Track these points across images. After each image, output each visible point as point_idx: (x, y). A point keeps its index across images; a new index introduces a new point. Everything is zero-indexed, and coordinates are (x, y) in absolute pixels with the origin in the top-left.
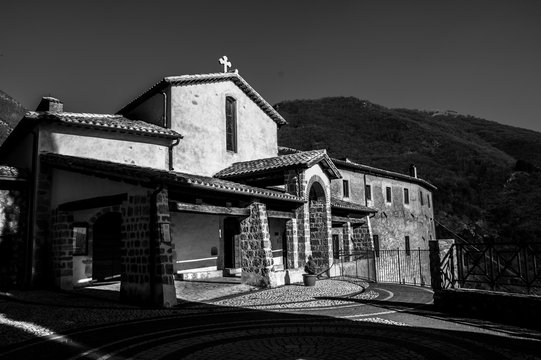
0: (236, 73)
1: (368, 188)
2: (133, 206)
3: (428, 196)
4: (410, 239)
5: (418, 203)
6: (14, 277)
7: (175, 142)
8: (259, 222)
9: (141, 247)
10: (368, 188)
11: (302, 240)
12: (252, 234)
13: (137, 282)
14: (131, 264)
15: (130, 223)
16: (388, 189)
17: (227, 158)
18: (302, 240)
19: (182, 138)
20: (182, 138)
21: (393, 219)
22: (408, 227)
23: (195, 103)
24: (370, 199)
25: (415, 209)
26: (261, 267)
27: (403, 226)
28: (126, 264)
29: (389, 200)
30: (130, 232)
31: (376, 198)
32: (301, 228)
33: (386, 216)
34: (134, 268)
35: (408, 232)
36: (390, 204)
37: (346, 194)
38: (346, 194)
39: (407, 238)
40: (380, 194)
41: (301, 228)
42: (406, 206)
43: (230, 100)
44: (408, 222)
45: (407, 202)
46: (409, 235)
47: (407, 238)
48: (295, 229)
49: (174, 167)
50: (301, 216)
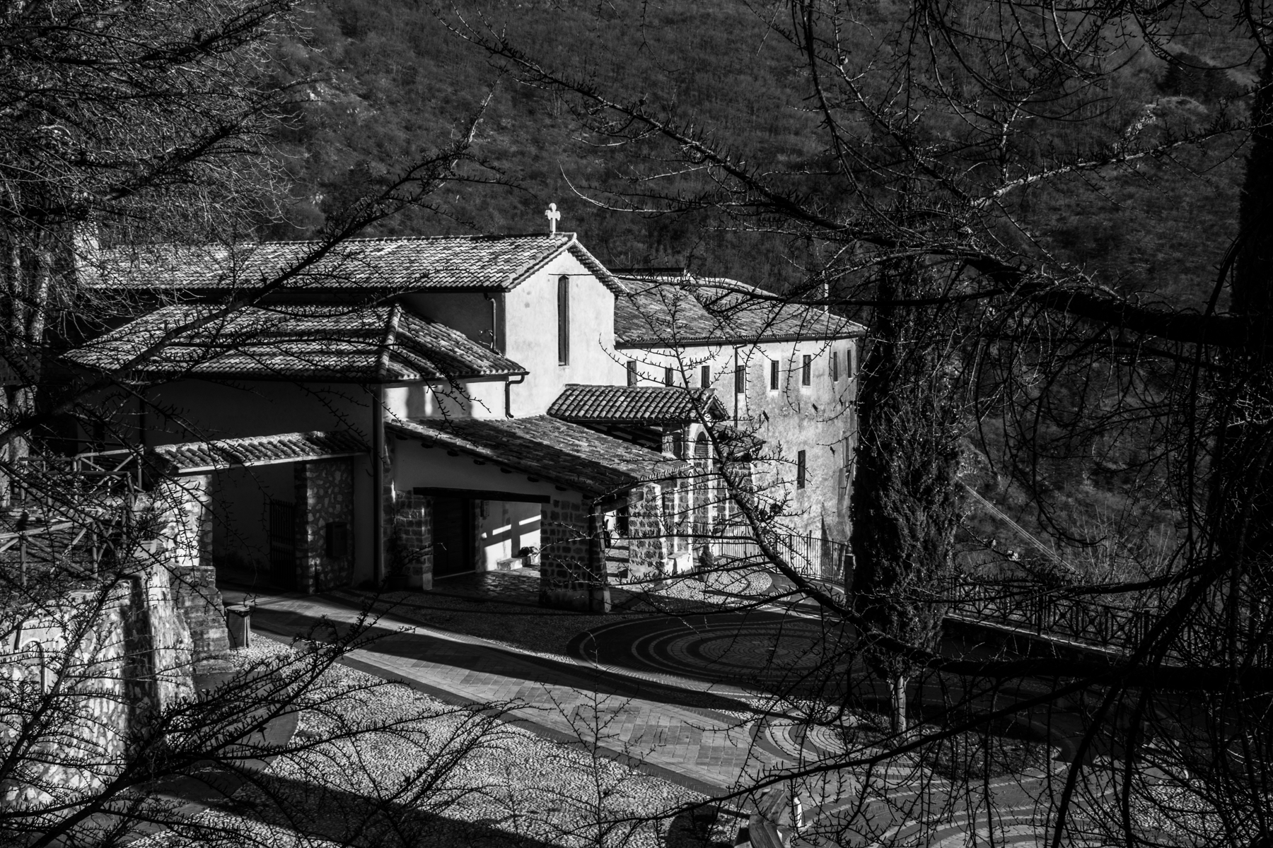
2: (558, 510)
3: (849, 352)
4: (807, 455)
5: (827, 380)
6: (344, 574)
7: (519, 378)
9: (572, 553)
12: (646, 520)
13: (566, 586)
14: (556, 570)
15: (554, 527)
16: (775, 365)
17: (560, 376)
19: (527, 373)
20: (527, 373)
21: (780, 420)
22: (804, 433)
23: (527, 305)
25: (821, 393)
26: (655, 560)
27: (797, 431)
28: (549, 569)
29: (774, 386)
30: (556, 537)
33: (767, 418)
35: (805, 443)
36: (775, 393)
39: (802, 454)
40: (761, 377)
42: (805, 391)
43: (563, 279)
44: (805, 423)
45: (806, 381)
46: (806, 448)
47: (802, 454)
49: (512, 412)
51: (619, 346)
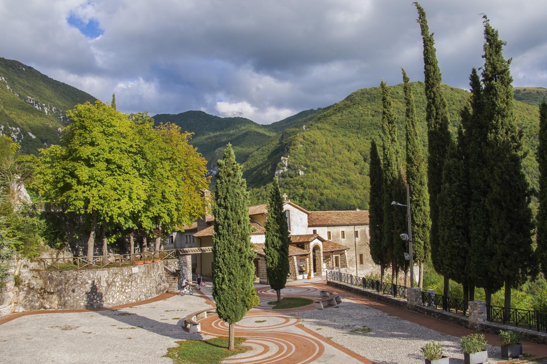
0: (289, 201)
1: (356, 233)
8: (294, 262)
10: (356, 233)
11: (310, 265)
18: (310, 265)
24: (358, 237)
26: (295, 274)
31: (361, 236)
32: (310, 261)
34: (263, 276)
37: (343, 237)
38: (343, 237)
41: (310, 261)
48: (308, 261)
50: (310, 257)
51: (309, 226)
